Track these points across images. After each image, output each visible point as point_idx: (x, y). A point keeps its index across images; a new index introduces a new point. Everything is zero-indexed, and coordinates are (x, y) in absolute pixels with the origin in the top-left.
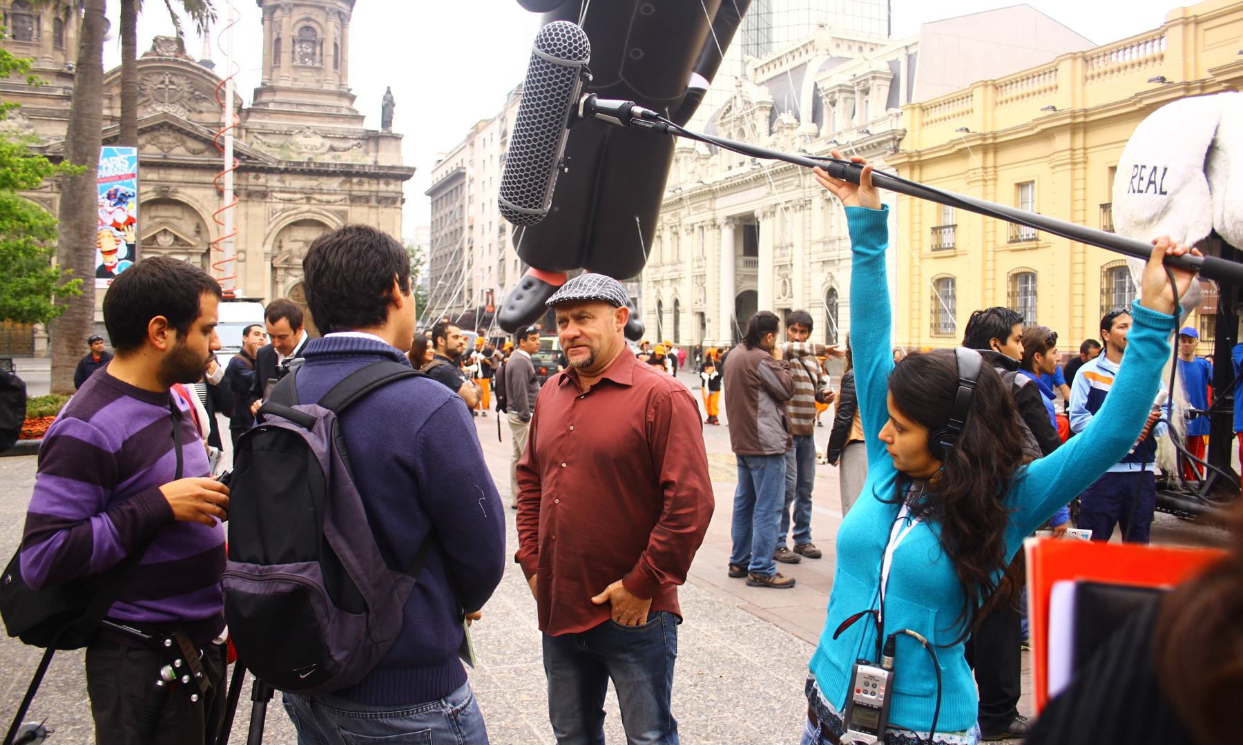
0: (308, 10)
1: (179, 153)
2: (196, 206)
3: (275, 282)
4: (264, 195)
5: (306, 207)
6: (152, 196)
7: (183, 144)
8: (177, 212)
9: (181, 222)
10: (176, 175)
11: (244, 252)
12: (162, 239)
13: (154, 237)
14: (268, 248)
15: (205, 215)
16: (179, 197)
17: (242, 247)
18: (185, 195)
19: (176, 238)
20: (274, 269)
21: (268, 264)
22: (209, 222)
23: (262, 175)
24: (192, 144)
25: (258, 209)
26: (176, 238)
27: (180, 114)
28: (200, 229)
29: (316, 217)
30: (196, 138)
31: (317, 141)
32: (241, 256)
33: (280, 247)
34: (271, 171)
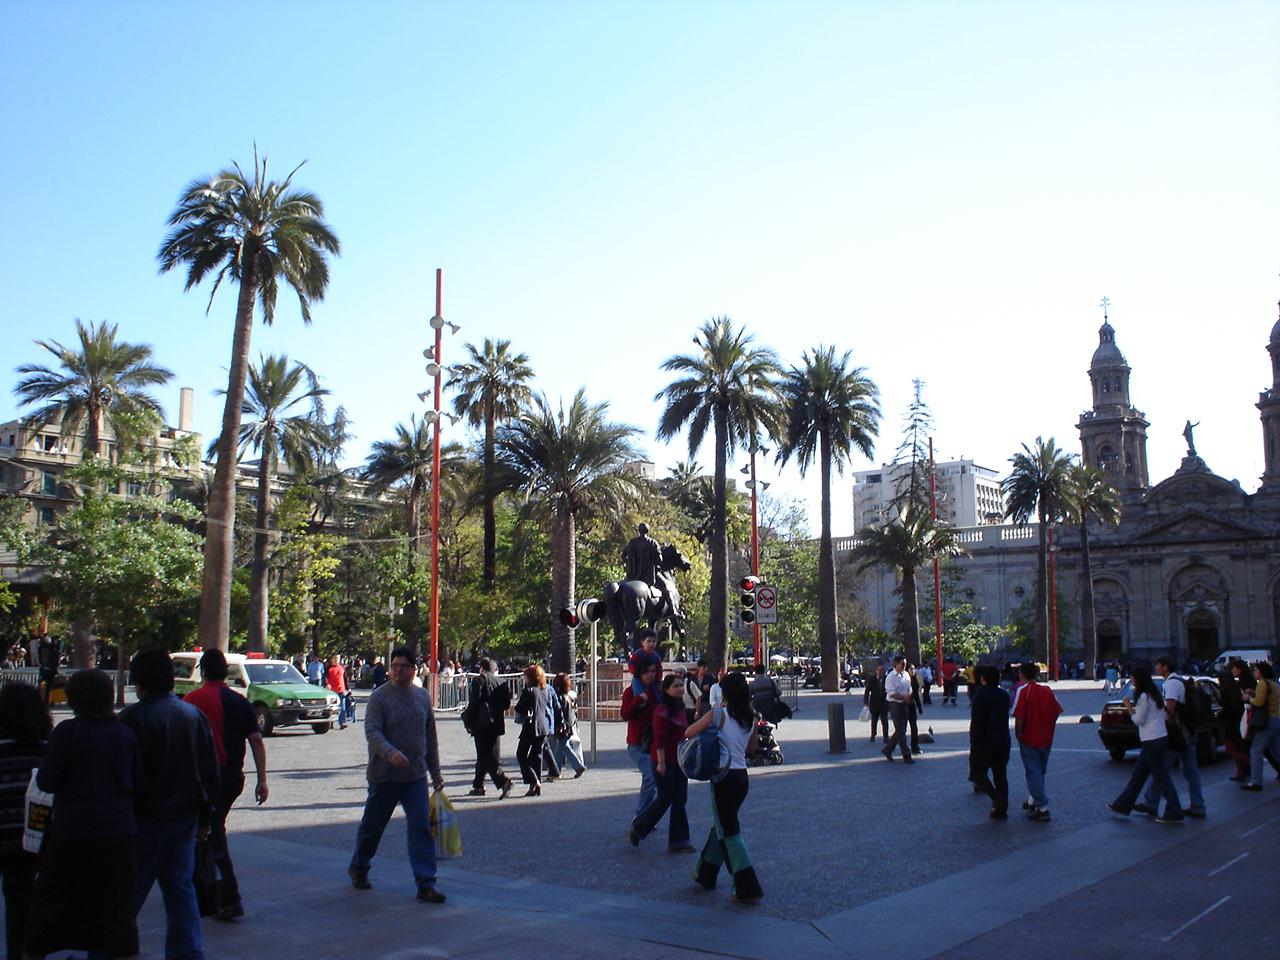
6: (1188, 563)
7: (1205, 526)
10: (1203, 548)
11: (1253, 596)
12: (1196, 591)
13: (1192, 590)
14: (1271, 592)
18: (1209, 560)
19: (1207, 590)
21: (1271, 604)
23: (1261, 542)
24: (1212, 526)
26: (1207, 590)
27: (1200, 507)
28: (1222, 582)
30: (1213, 521)
34: (1266, 539)
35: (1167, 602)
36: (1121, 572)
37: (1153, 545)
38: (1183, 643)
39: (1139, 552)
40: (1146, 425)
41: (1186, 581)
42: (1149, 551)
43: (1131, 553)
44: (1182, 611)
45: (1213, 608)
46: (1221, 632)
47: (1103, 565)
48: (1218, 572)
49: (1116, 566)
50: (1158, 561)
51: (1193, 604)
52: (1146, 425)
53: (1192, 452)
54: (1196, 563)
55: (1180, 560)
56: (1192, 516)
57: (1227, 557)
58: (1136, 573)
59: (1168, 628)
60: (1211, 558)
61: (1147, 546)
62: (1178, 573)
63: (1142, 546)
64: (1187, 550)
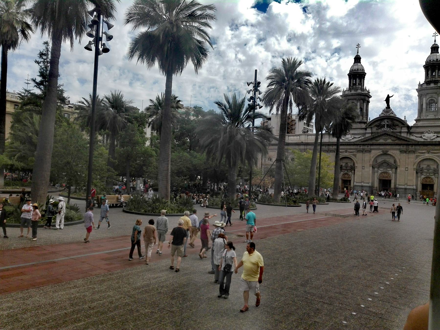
0: (430, 95)
1: (389, 141)
2: (394, 155)
3: (417, 177)
4: (414, 152)
5: (427, 155)
6: (382, 153)
8: (389, 157)
9: (390, 160)
10: (388, 147)
11: (407, 168)
14: (415, 167)
15: (396, 158)
16: (389, 153)
17: (407, 167)
20: (417, 173)
21: (415, 172)
22: (397, 160)
25: (412, 156)
28: (395, 162)
29: (431, 158)
31: (432, 135)
32: (407, 169)
33: (420, 167)
35: (371, 168)
36: (354, 155)
37: (368, 145)
38: (376, 184)
39: (362, 147)
40: (370, 97)
41: (380, 160)
42: (366, 147)
43: (358, 147)
44: (377, 172)
45: (390, 171)
46: (393, 182)
47: (346, 152)
48: (394, 157)
49: (351, 152)
50: (370, 151)
51: (382, 169)
52: (370, 97)
53: (388, 107)
54: (385, 154)
55: (379, 151)
56: (386, 134)
57: (398, 152)
58: (359, 155)
59: (371, 178)
60: (392, 151)
61: (366, 145)
62: (376, 157)
63: (363, 145)
64: (382, 147)
